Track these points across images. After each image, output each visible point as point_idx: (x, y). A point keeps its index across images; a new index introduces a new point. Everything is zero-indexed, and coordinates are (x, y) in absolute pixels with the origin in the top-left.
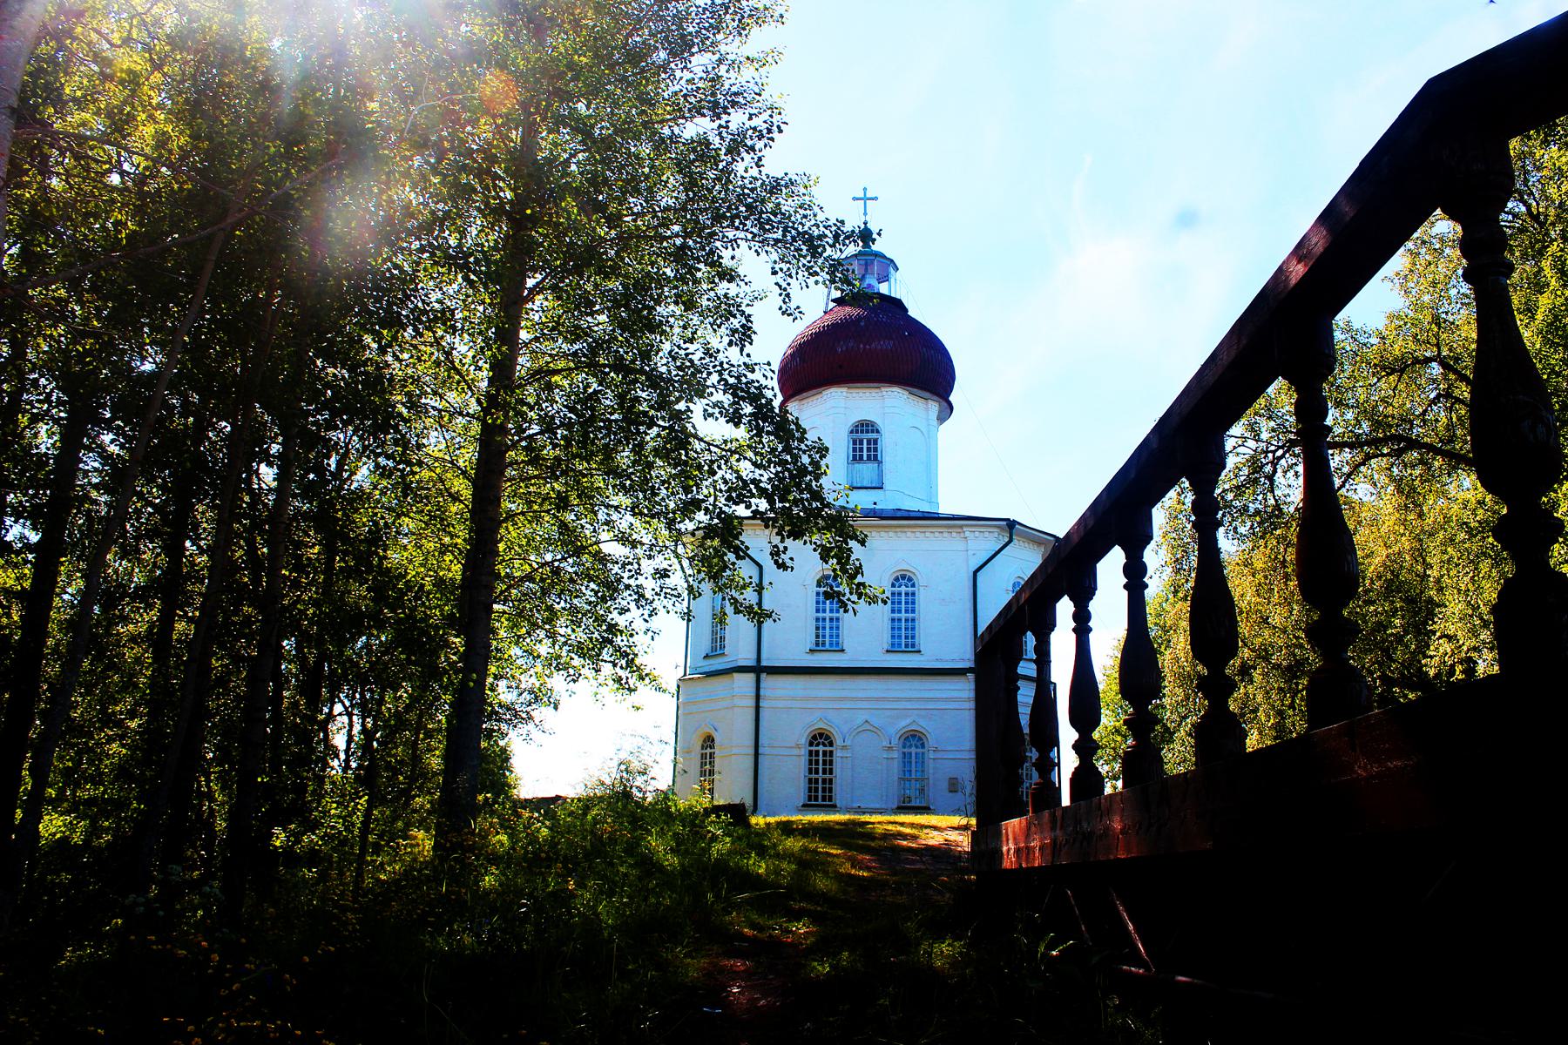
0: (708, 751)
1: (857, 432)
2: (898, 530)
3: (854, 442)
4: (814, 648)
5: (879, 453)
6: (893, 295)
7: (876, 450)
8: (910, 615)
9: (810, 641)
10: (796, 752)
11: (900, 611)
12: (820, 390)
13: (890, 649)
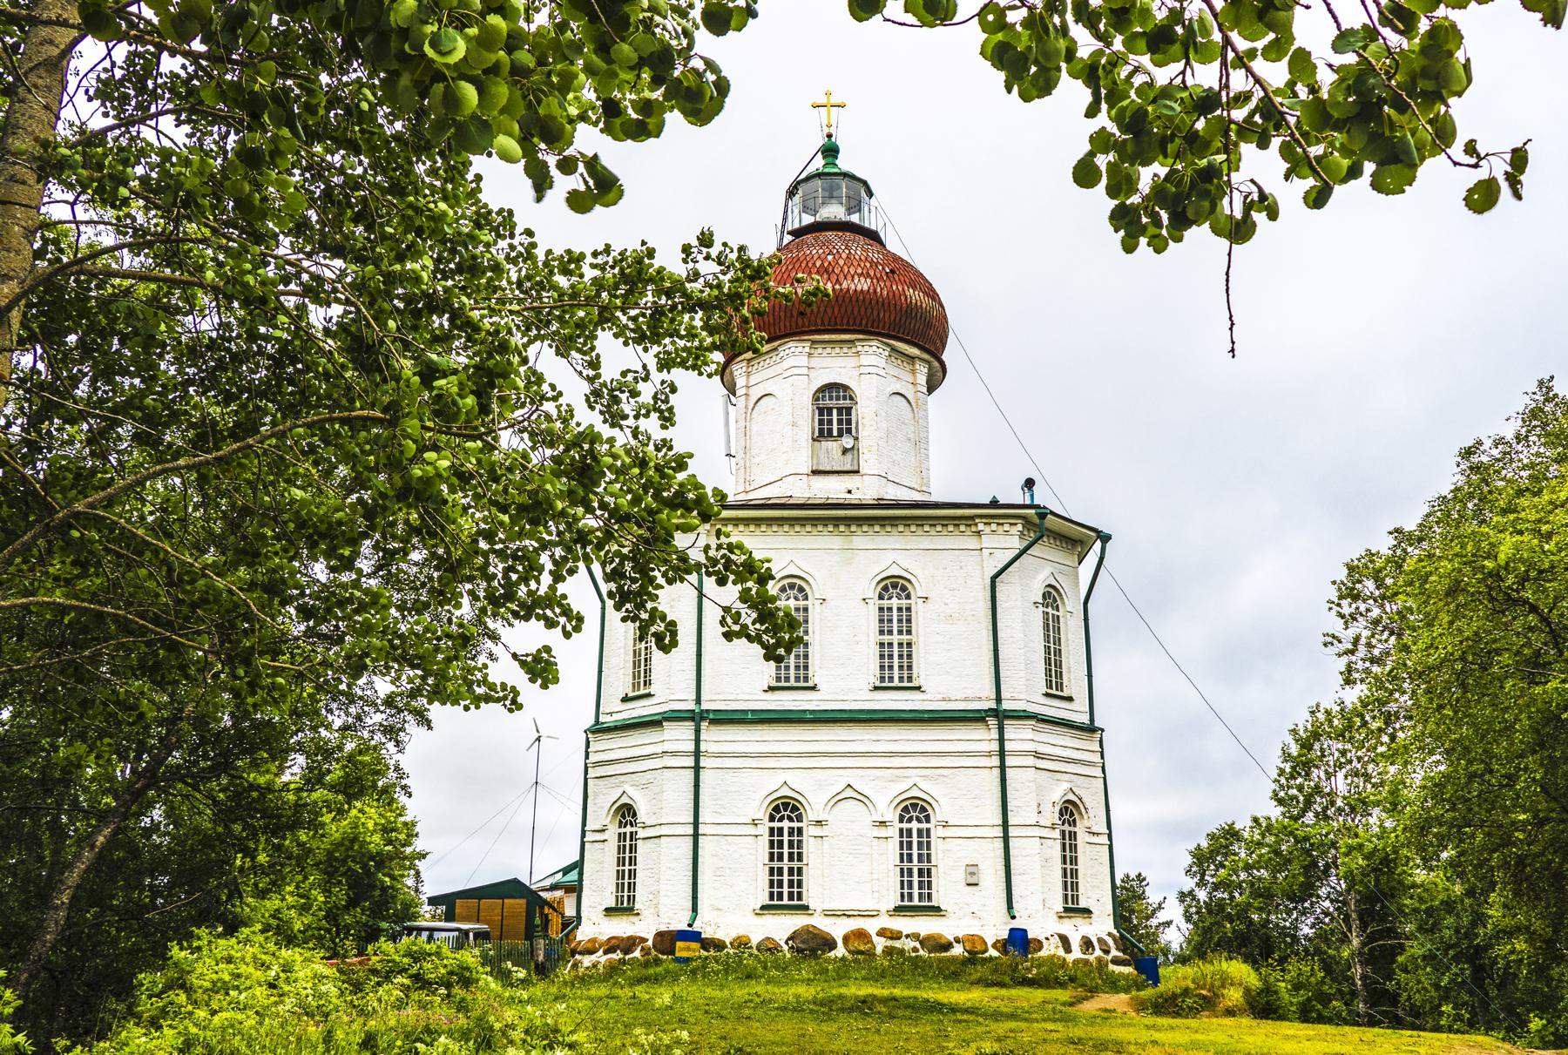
0: (629, 829)
3: (821, 411)
4: (774, 684)
5: (853, 426)
6: (867, 225)
10: (751, 830)
11: (890, 632)
13: (878, 684)
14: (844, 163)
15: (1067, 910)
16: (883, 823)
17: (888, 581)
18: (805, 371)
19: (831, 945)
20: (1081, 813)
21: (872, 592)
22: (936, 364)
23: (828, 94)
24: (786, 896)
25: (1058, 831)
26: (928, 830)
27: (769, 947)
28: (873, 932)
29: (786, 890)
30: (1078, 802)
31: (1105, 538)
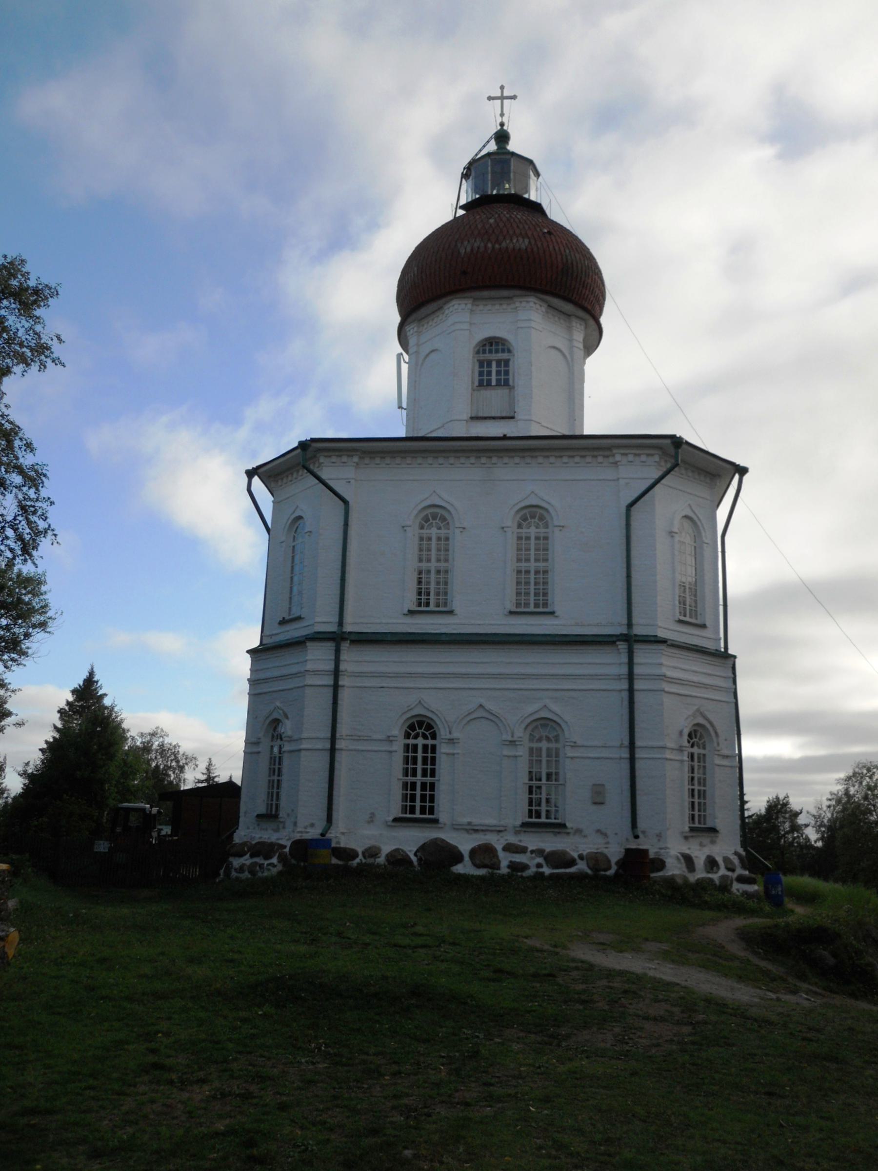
1: (484, 352)
3: (481, 363)
5: (511, 377)
7: (507, 373)
8: (541, 565)
9: (410, 601)
12: (440, 302)
13: (514, 609)
14: (512, 146)
15: (692, 829)
16: (512, 743)
17: (526, 511)
18: (466, 326)
19: (458, 857)
20: (710, 735)
21: (510, 522)
22: (592, 322)
23: (502, 88)
25: (686, 753)
27: (398, 859)
28: (499, 848)
29: (418, 804)
30: (708, 726)
31: (743, 471)
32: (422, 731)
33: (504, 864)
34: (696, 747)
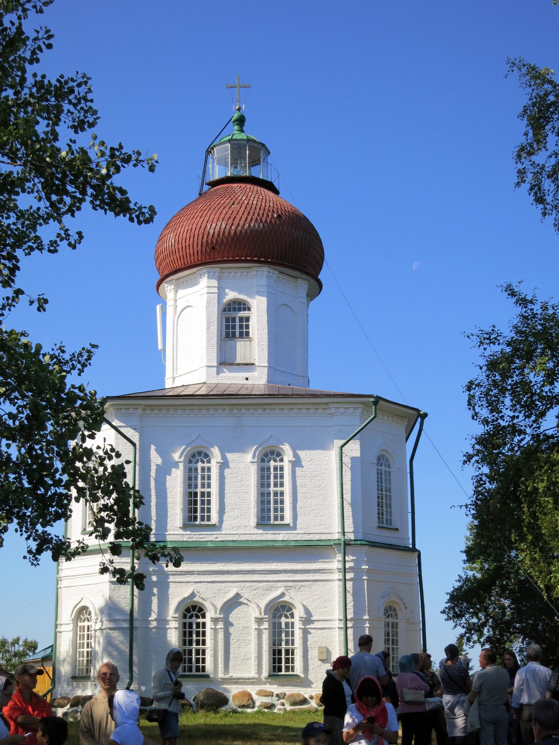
2: (267, 407)
3: (227, 320)
22: (313, 282)
24: (194, 669)
26: (293, 624)
32: (196, 612)
33: (258, 704)
34: (390, 618)
